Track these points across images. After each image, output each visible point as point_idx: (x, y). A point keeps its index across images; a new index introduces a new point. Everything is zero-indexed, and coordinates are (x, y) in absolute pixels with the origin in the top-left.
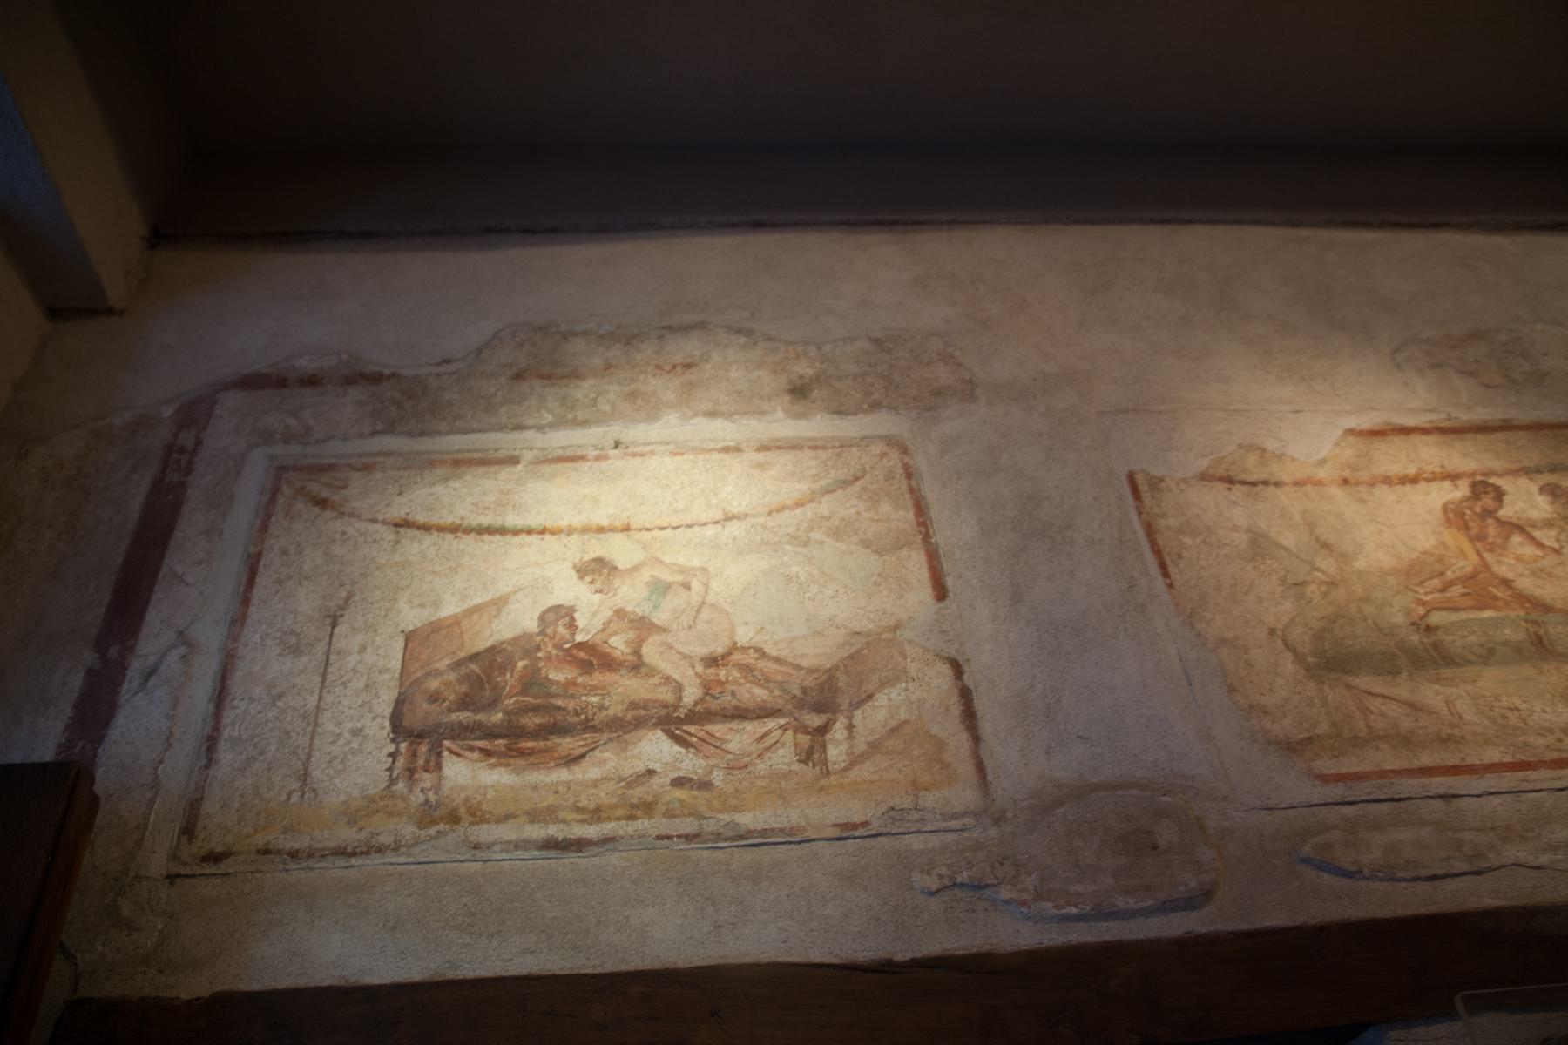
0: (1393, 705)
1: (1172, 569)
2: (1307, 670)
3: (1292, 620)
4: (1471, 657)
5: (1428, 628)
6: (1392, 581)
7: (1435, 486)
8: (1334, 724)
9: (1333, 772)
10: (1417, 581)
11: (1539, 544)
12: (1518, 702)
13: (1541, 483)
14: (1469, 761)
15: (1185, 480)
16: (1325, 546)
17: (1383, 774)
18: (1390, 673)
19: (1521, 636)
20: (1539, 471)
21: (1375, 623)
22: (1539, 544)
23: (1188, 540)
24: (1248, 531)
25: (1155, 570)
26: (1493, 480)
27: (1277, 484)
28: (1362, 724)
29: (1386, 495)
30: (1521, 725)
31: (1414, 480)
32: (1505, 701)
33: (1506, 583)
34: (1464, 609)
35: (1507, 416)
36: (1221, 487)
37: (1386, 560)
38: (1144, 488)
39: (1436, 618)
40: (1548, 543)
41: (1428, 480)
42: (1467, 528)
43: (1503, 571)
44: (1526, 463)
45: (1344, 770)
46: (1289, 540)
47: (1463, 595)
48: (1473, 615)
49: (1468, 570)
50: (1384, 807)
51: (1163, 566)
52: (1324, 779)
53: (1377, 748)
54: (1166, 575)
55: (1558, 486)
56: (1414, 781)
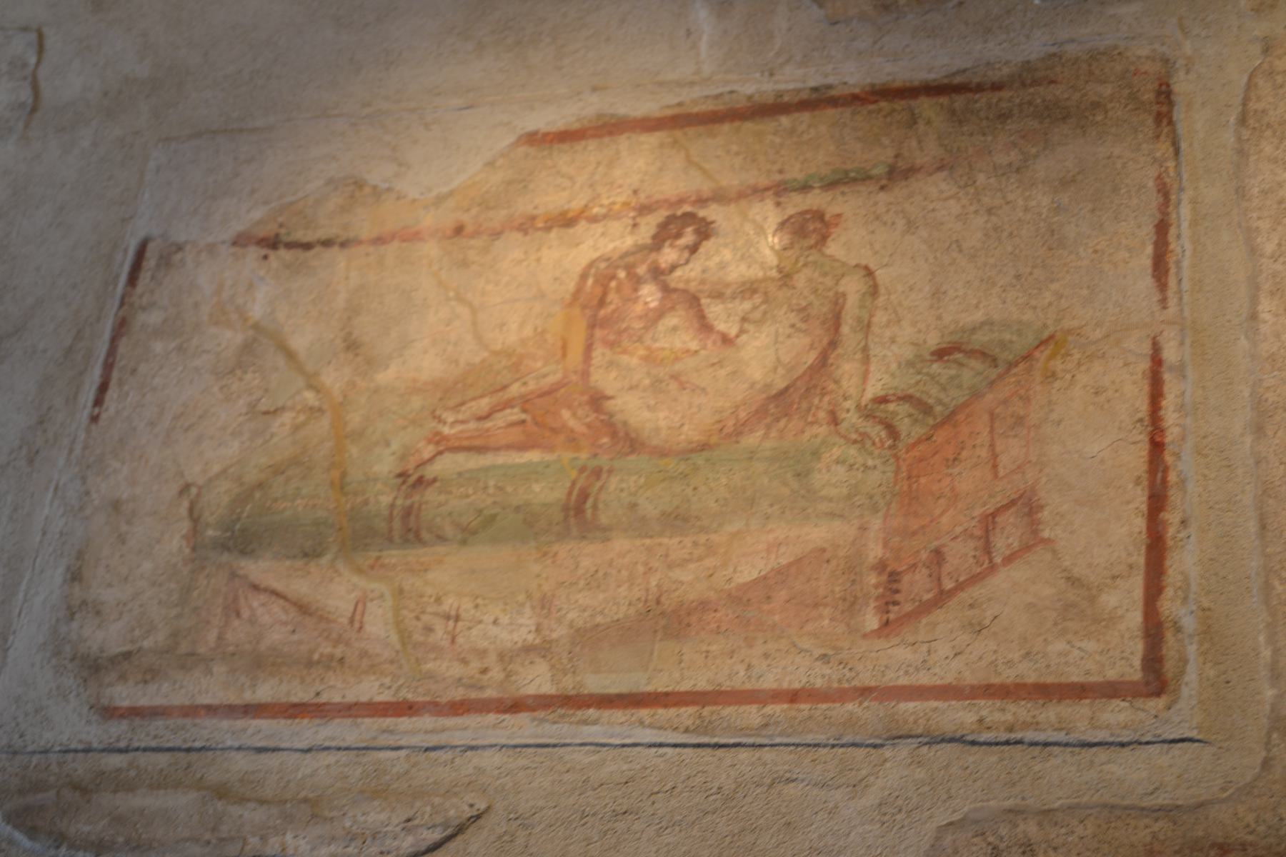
0: (277, 607)
1: (112, 394)
2: (194, 549)
3: (224, 471)
4: (449, 531)
5: (420, 480)
6: (416, 402)
7: (598, 228)
8: (175, 634)
9: (126, 703)
10: (452, 403)
11: (704, 326)
12: (467, 605)
13: (791, 211)
14: (324, 698)
15: (211, 249)
16: (352, 346)
17: (191, 711)
18: (306, 555)
19: (559, 494)
20: (805, 188)
21: (344, 475)
22: (704, 326)
23: (158, 347)
24: (256, 327)
25: (89, 394)
26: (712, 212)
27: (344, 245)
28: (212, 636)
29: (512, 250)
30: (445, 643)
31: (566, 221)
32: (449, 604)
33: (597, 400)
34: (497, 449)
35: (831, 80)
36: (254, 252)
37: (428, 364)
38: (150, 262)
39: (447, 465)
40: (721, 326)
41: (594, 219)
42: (602, 303)
43: (604, 380)
44: (795, 173)
45: (143, 702)
46: (299, 343)
47: (512, 425)
48: (501, 459)
49: (552, 379)
50: (163, 759)
51: (103, 388)
52: (109, 713)
53: (209, 672)
54: (98, 402)
55: (819, 216)
56: (225, 724)
